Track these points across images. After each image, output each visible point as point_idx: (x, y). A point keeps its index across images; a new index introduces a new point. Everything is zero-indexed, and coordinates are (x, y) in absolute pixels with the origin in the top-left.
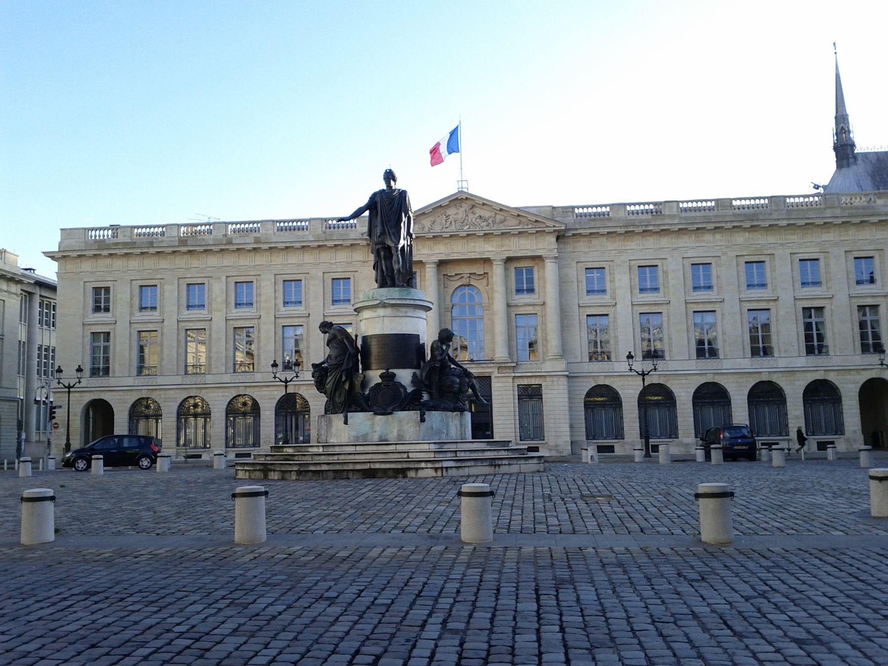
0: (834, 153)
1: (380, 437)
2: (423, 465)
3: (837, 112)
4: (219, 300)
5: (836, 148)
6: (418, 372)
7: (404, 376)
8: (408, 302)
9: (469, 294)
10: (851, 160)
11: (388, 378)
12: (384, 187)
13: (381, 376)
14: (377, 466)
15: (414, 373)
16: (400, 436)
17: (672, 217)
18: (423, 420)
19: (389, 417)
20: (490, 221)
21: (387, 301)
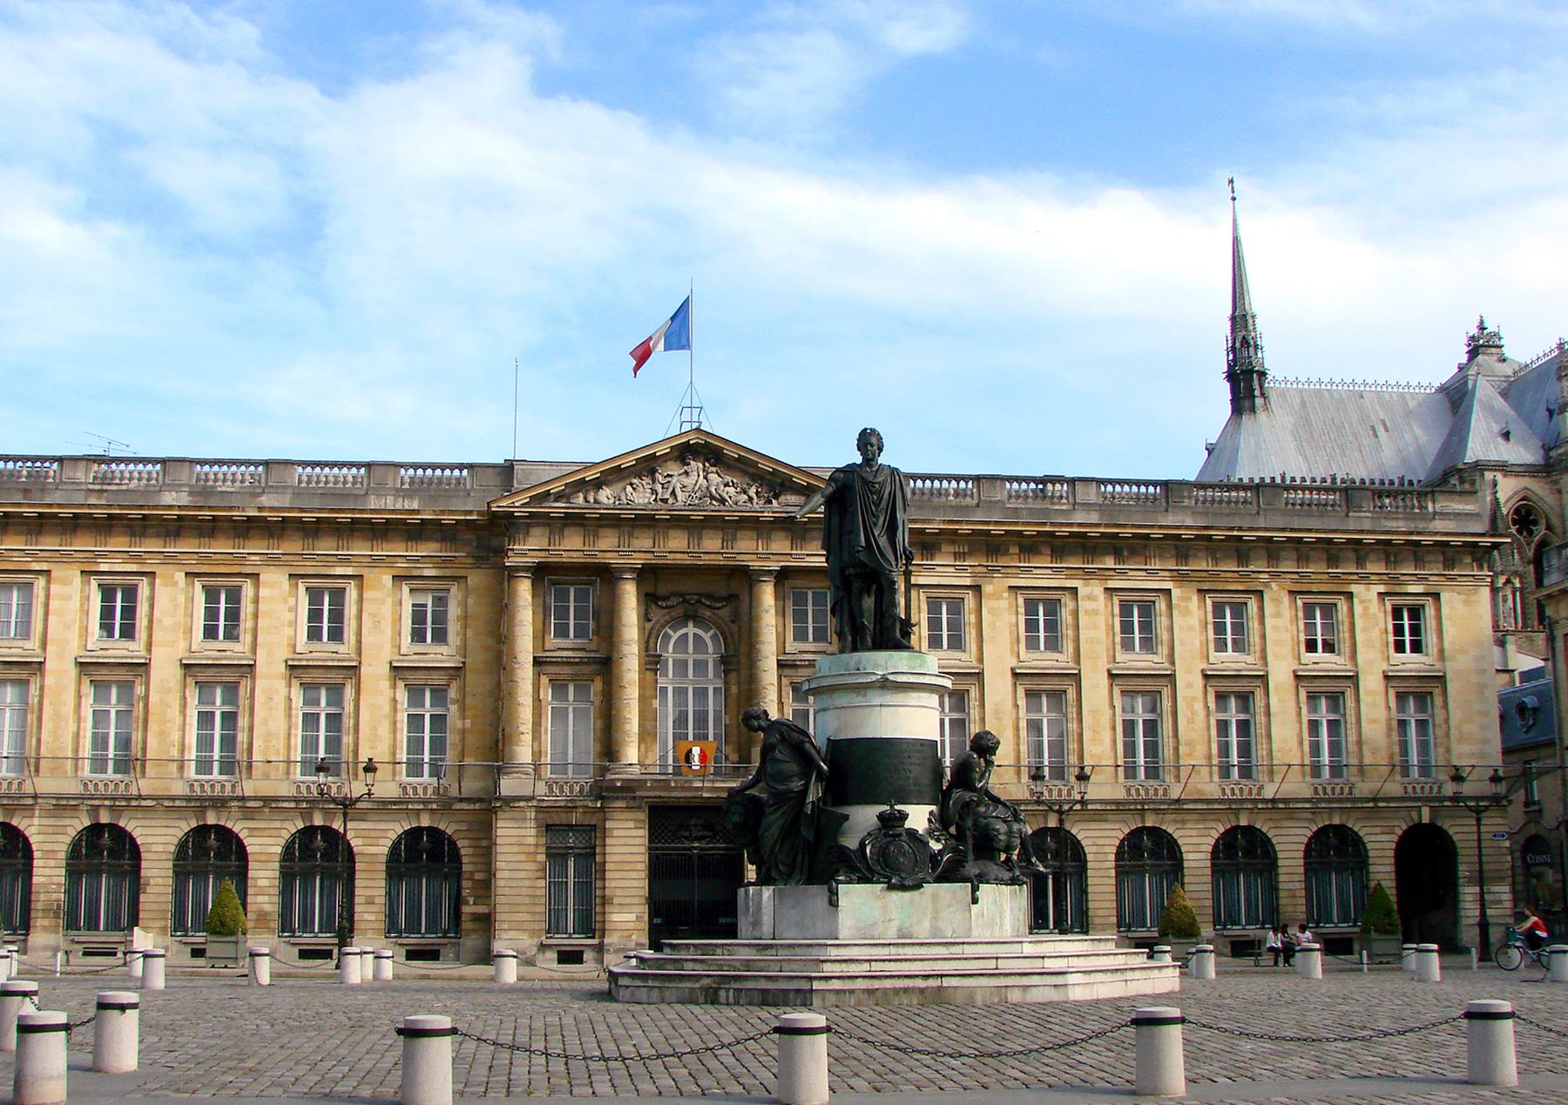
0: (1228, 385)
1: (900, 930)
2: (1035, 980)
3: (1234, 308)
4: (168, 621)
5: (1231, 376)
6: (933, 808)
7: (918, 817)
8: (921, 680)
10: (1259, 401)
11: (891, 821)
12: (858, 459)
13: (881, 817)
14: (954, 982)
15: (931, 813)
16: (935, 931)
17: (1088, 506)
18: (975, 901)
19: (915, 894)
20: (752, 491)
21: (891, 678)
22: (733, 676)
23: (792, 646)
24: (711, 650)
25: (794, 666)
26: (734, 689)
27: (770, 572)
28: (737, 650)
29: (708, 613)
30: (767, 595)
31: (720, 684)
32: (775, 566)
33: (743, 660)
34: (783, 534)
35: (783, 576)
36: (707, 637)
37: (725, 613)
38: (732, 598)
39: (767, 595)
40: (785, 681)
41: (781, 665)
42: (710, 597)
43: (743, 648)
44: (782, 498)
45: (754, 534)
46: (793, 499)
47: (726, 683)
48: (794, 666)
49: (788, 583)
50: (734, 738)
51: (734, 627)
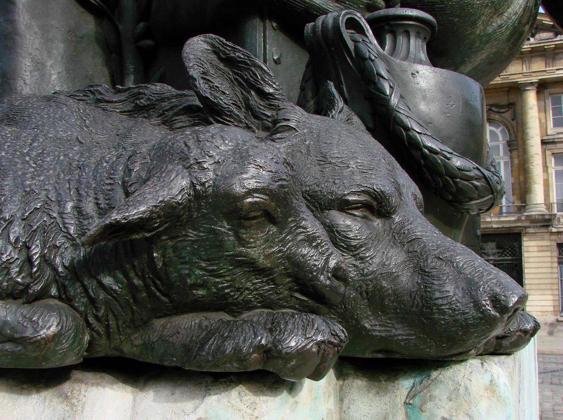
9: (491, 131)
22: (515, 153)
23: (551, 130)
24: (501, 139)
25: (553, 143)
26: (516, 161)
27: (532, 84)
28: (516, 137)
29: (497, 117)
30: (531, 98)
31: (507, 159)
32: (535, 79)
33: (520, 142)
34: (539, 59)
35: (542, 87)
36: (498, 131)
37: (508, 115)
38: (511, 105)
39: (531, 98)
40: (548, 153)
41: (543, 143)
42: (497, 106)
43: (519, 135)
44: (537, 36)
45: (520, 61)
46: (544, 35)
47: (511, 158)
48: (553, 143)
49: (547, 92)
50: (517, 192)
51: (514, 123)
